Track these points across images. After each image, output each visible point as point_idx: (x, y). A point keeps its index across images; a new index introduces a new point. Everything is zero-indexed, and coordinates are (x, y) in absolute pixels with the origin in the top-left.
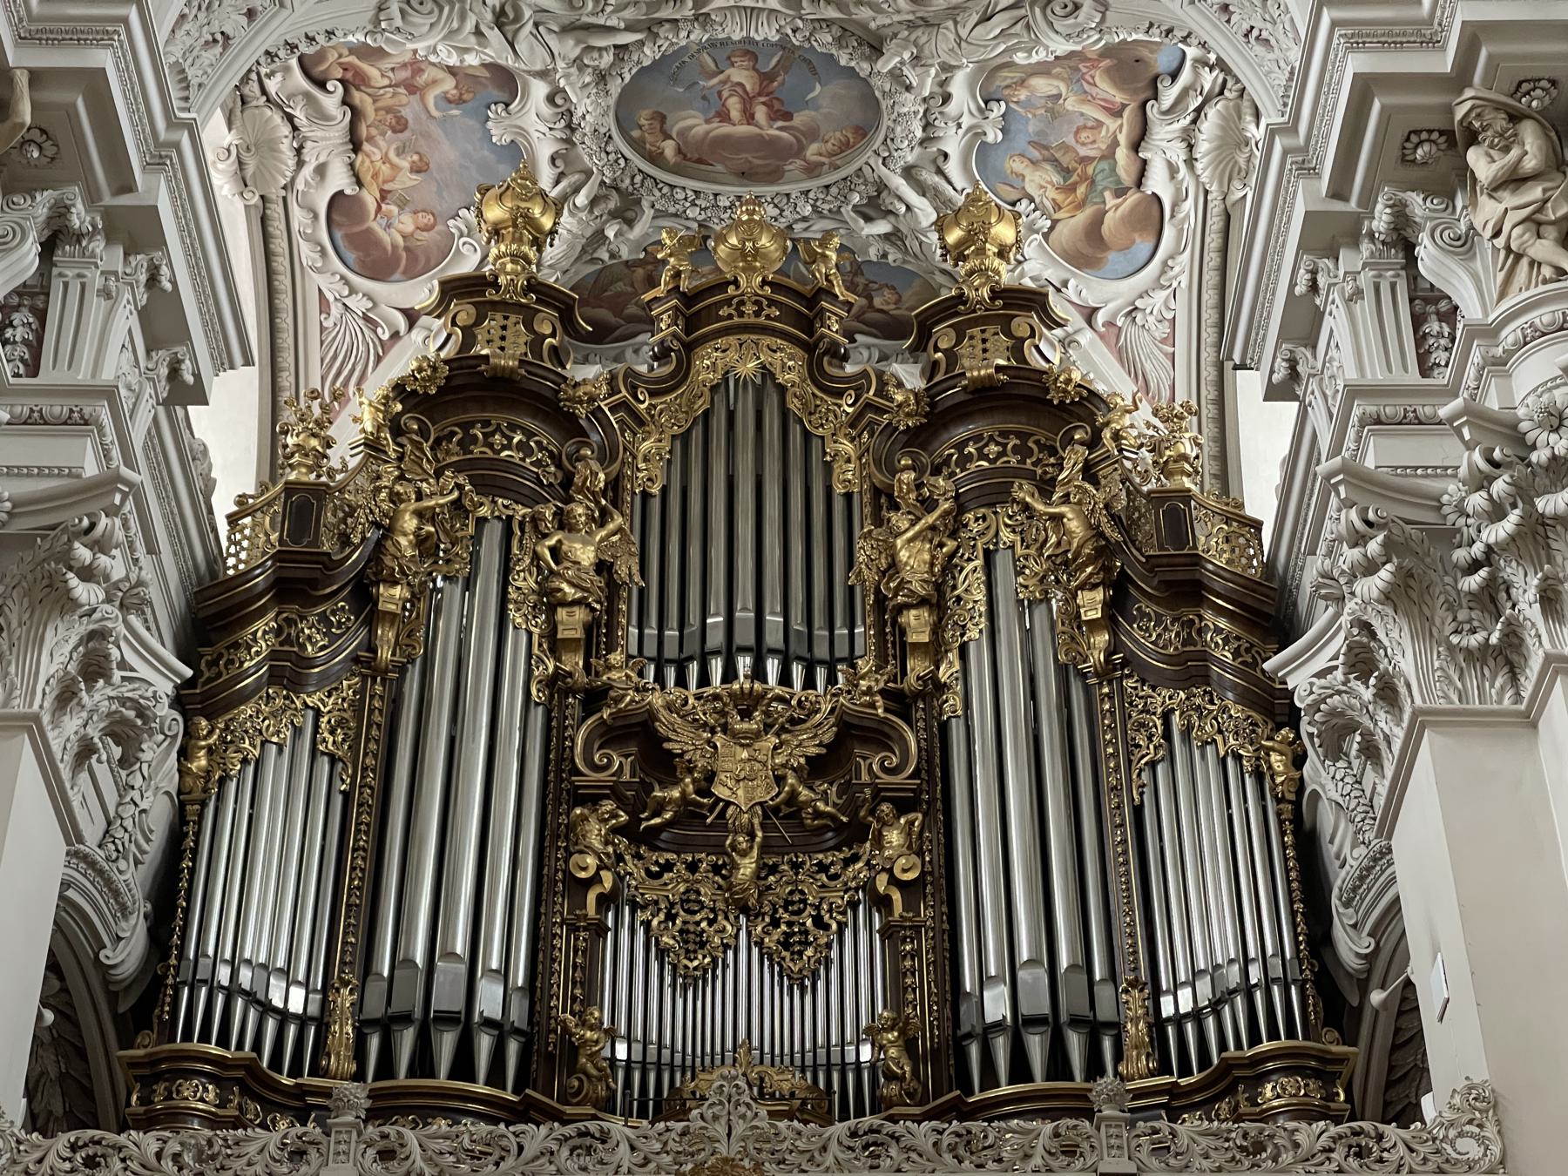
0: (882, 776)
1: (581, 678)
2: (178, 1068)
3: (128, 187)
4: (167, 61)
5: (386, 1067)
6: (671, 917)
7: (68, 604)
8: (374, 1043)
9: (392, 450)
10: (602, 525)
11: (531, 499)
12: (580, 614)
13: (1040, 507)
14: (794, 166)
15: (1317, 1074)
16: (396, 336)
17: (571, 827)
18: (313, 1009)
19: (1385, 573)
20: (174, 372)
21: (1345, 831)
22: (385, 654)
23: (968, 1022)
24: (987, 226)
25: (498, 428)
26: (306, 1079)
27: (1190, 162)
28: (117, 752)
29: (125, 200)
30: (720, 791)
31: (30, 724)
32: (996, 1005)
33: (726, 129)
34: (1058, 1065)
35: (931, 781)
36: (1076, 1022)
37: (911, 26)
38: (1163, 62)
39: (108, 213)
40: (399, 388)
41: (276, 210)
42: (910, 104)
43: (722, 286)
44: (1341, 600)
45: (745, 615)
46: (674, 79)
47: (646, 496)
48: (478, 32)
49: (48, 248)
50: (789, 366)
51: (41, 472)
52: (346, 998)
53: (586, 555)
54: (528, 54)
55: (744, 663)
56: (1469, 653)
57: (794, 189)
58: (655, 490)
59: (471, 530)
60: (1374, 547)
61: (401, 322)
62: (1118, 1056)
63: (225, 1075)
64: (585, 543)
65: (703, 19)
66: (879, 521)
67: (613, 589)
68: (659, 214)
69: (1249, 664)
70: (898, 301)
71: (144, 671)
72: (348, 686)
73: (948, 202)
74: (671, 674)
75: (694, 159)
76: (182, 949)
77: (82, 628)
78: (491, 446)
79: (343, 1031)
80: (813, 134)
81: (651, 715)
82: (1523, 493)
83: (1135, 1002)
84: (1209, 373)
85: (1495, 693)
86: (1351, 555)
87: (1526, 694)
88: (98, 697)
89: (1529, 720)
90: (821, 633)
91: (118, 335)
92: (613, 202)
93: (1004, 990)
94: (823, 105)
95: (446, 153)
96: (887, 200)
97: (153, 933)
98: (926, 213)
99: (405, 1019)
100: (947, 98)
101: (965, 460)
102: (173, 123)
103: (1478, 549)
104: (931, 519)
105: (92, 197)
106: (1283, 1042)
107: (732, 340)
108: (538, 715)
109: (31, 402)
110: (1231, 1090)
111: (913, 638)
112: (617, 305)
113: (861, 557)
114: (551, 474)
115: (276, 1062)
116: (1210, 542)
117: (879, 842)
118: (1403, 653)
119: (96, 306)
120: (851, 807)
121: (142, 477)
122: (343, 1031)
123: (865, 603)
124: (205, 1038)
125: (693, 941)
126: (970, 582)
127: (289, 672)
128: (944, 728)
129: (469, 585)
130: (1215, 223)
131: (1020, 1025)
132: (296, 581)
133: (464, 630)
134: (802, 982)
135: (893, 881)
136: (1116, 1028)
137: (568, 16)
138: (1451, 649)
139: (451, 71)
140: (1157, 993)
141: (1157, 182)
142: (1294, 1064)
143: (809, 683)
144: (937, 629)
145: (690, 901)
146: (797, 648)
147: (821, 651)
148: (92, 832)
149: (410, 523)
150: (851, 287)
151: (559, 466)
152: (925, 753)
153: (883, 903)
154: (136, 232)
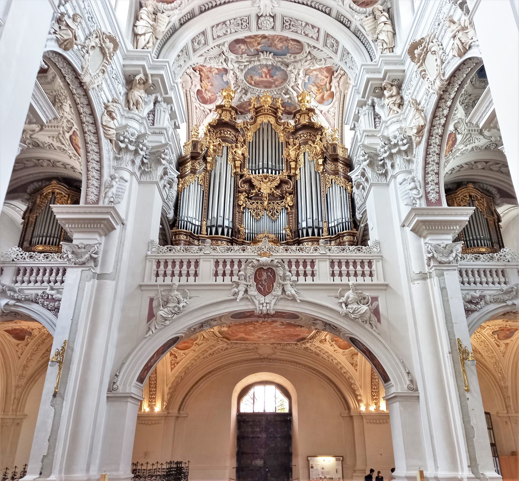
0: (287, 188)
1: (240, 173)
2: (180, 233)
4: (172, 70)
5: (211, 234)
6: (254, 211)
7: (160, 163)
8: (209, 230)
9: (209, 134)
10: (242, 147)
11: (231, 143)
12: (239, 162)
13: (313, 145)
14: (273, 86)
15: (352, 236)
16: (208, 114)
17: (238, 197)
18: (200, 224)
19: (368, 161)
20: (175, 124)
21: (359, 199)
22: (209, 168)
23: (300, 227)
24: (305, 97)
26: (199, 235)
27: (339, 86)
28: (169, 186)
29: (167, 96)
30: (261, 191)
31: (157, 183)
32: (304, 225)
33: (262, 79)
34: (313, 234)
35: (294, 190)
36: (316, 227)
37: (293, 62)
38: (335, 69)
39: (164, 98)
40: (210, 124)
41: (188, 92)
42: (293, 75)
43: (262, 107)
44: (360, 165)
45: (265, 162)
46: (254, 70)
47: (249, 142)
48: (222, 63)
49: (155, 104)
50: (272, 120)
51: (156, 142)
52: (204, 223)
53: (240, 152)
54: (230, 66)
55: (265, 170)
56: (380, 174)
57: (273, 89)
58: (251, 141)
60: (366, 157)
61: (209, 111)
62: (322, 233)
63: (187, 234)
65: (259, 61)
66: (287, 147)
67: (244, 158)
68: (251, 93)
69: (345, 173)
70: (290, 109)
71: (173, 173)
72: (203, 173)
73: (299, 92)
74: (254, 172)
75: (257, 84)
76: (179, 215)
77: (163, 167)
79: (204, 228)
80: (277, 80)
81: (251, 179)
82: (390, 149)
83: (325, 225)
84: (340, 125)
85: (383, 180)
86: (363, 158)
87: (388, 180)
88: (166, 178)
89: (388, 185)
90: (277, 165)
91: (166, 119)
92: (244, 91)
93: (305, 222)
94: (278, 75)
95: (216, 83)
96: (289, 92)
97: (174, 212)
98: (295, 94)
99: (214, 226)
100: (299, 75)
101: (301, 137)
102: (174, 82)
103: (382, 158)
104: (295, 147)
105: (161, 95)
106: (348, 231)
107: (263, 116)
108: (233, 179)
109: (154, 130)
110: (339, 238)
111: (292, 167)
112: (244, 109)
113: (284, 153)
114: (234, 139)
115: (194, 232)
116: (340, 152)
117: (286, 199)
118: (369, 173)
119: (163, 113)
120: (282, 194)
121: (171, 143)
122: (204, 228)
123: (284, 161)
124: (183, 229)
125: (258, 214)
126: (301, 157)
127: (194, 171)
128: (297, 181)
129: (222, 156)
130: (342, 96)
131: (307, 228)
132: (194, 157)
133: (221, 164)
134: (274, 221)
135: (289, 205)
136: (322, 228)
137: (236, 60)
138: (377, 173)
139: (217, 69)
140: (329, 223)
141: (333, 89)
142: (349, 234)
143: (276, 174)
144: (296, 165)
145: (257, 208)
146: (274, 168)
147: (277, 168)
148: (165, 197)
149: (212, 147)
150: (282, 107)
152: (294, 186)
153: (287, 209)
154: (168, 101)
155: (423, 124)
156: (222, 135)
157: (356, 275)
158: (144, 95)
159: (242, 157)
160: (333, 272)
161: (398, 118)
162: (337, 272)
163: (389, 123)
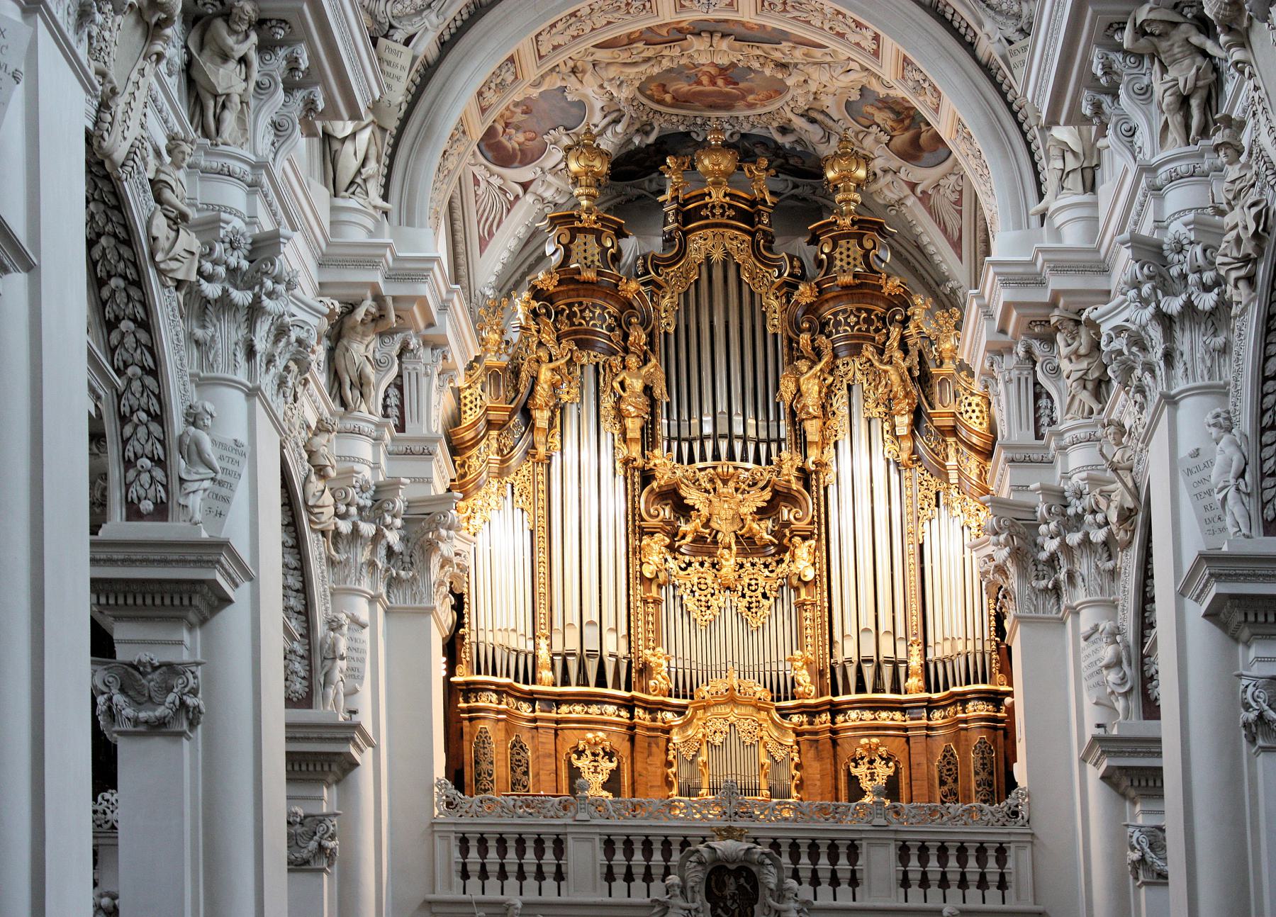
3: (430, 325)
9: (533, 327)
10: (646, 361)
25: (587, 307)
29: (431, 331)
47: (666, 334)
49: (400, 356)
58: (671, 330)
59: (579, 372)
62: (907, 676)
64: (637, 378)
67: (653, 403)
78: (584, 318)
102: (450, 291)
105: (417, 333)
151: (620, 326)
155: (1132, 506)
156: (576, 321)
157: (963, 884)
158: (373, 341)
159: (643, 400)
160: (905, 873)
161: (1089, 430)
162: (915, 876)
163: (1068, 438)
